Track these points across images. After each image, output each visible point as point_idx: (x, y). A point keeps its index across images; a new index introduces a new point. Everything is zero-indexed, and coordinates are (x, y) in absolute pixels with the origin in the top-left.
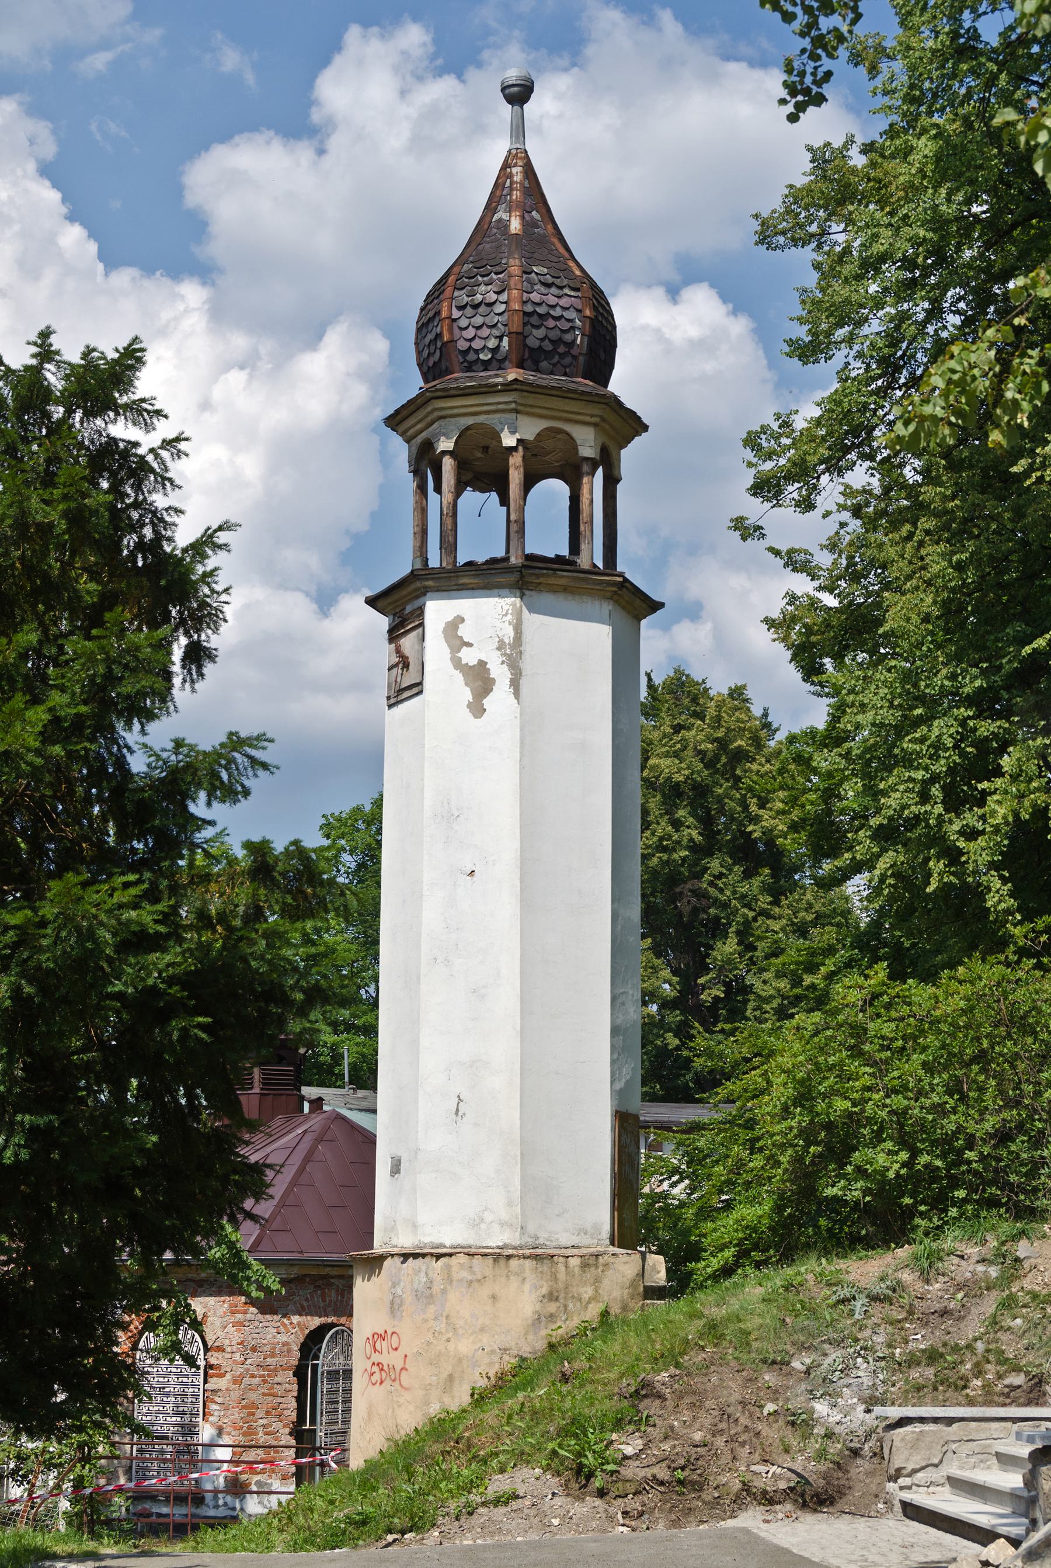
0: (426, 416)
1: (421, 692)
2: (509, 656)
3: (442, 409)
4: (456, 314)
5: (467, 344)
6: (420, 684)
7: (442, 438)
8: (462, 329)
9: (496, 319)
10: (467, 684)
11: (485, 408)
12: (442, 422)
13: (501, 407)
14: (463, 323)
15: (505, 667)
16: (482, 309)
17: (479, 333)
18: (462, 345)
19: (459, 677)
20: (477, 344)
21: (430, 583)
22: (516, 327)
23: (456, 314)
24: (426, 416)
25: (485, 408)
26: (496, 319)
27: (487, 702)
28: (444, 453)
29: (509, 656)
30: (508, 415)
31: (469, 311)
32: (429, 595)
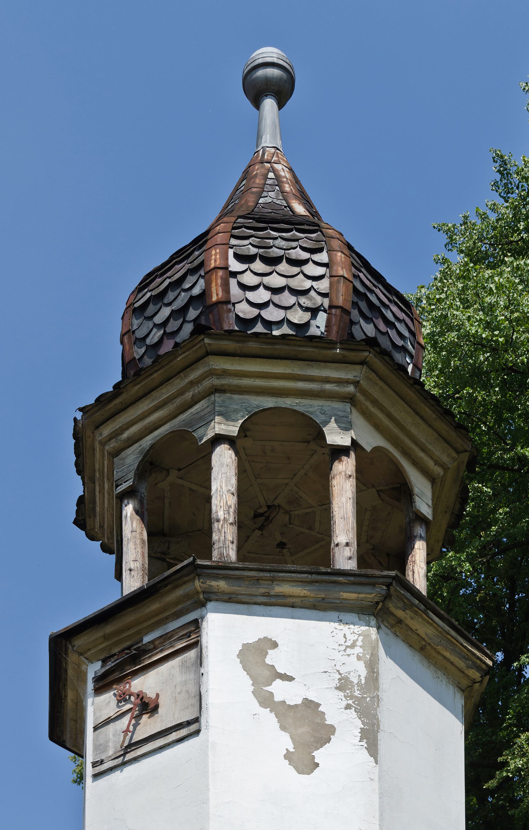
0: (181, 392)
1: (197, 732)
2: (359, 701)
3: (225, 373)
4: (235, 266)
5: (255, 312)
6: (197, 720)
7: (218, 419)
8: (244, 287)
9: (308, 284)
10: (283, 728)
11: (300, 385)
12: (218, 398)
13: (328, 387)
14: (249, 279)
15: (352, 714)
16: (283, 267)
17: (276, 299)
18: (245, 311)
19: (269, 719)
20: (272, 314)
21: (222, 585)
22: (342, 298)
23: (235, 266)
24: (181, 392)
25: (300, 385)
26: (308, 284)
27: (319, 755)
28: (219, 439)
29: (359, 701)
30: (337, 405)
31: (258, 266)
32: (210, 605)
